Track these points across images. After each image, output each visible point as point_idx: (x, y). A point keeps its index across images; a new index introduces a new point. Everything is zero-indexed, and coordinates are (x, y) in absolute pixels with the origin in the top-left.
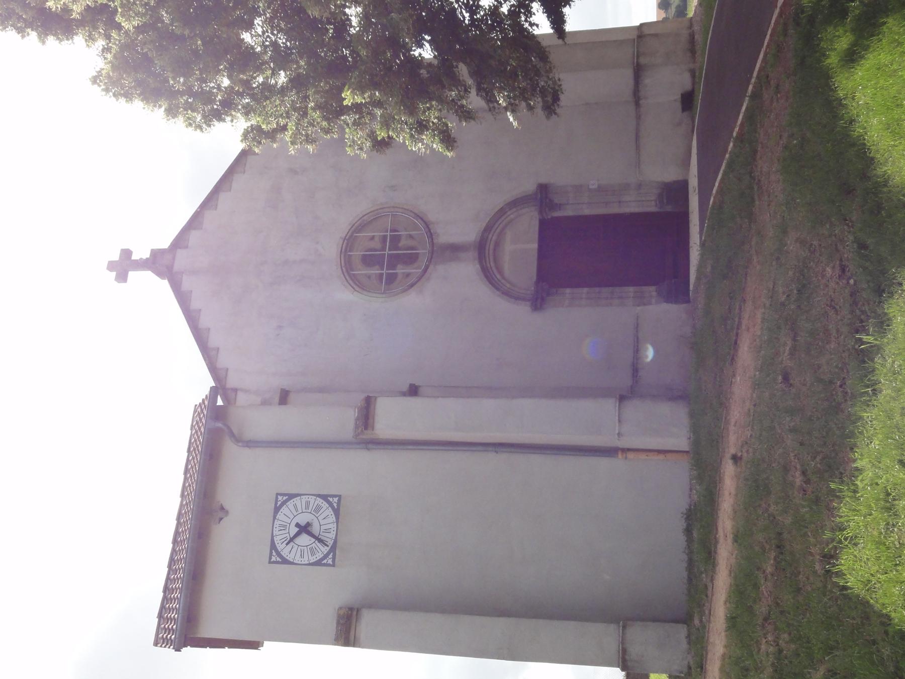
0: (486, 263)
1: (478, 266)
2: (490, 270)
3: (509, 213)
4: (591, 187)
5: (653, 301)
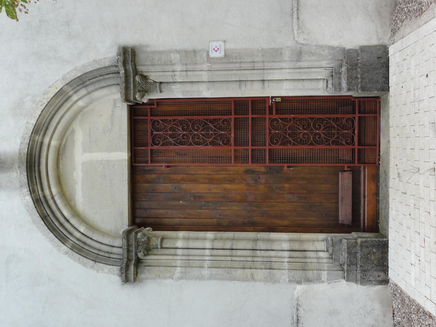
0: (42, 190)
1: (29, 199)
2: (51, 202)
3: (75, 98)
4: (213, 54)
5: (324, 275)
